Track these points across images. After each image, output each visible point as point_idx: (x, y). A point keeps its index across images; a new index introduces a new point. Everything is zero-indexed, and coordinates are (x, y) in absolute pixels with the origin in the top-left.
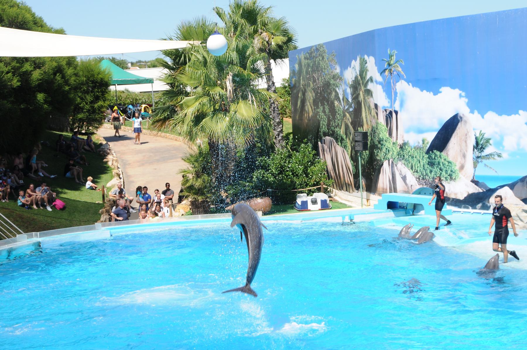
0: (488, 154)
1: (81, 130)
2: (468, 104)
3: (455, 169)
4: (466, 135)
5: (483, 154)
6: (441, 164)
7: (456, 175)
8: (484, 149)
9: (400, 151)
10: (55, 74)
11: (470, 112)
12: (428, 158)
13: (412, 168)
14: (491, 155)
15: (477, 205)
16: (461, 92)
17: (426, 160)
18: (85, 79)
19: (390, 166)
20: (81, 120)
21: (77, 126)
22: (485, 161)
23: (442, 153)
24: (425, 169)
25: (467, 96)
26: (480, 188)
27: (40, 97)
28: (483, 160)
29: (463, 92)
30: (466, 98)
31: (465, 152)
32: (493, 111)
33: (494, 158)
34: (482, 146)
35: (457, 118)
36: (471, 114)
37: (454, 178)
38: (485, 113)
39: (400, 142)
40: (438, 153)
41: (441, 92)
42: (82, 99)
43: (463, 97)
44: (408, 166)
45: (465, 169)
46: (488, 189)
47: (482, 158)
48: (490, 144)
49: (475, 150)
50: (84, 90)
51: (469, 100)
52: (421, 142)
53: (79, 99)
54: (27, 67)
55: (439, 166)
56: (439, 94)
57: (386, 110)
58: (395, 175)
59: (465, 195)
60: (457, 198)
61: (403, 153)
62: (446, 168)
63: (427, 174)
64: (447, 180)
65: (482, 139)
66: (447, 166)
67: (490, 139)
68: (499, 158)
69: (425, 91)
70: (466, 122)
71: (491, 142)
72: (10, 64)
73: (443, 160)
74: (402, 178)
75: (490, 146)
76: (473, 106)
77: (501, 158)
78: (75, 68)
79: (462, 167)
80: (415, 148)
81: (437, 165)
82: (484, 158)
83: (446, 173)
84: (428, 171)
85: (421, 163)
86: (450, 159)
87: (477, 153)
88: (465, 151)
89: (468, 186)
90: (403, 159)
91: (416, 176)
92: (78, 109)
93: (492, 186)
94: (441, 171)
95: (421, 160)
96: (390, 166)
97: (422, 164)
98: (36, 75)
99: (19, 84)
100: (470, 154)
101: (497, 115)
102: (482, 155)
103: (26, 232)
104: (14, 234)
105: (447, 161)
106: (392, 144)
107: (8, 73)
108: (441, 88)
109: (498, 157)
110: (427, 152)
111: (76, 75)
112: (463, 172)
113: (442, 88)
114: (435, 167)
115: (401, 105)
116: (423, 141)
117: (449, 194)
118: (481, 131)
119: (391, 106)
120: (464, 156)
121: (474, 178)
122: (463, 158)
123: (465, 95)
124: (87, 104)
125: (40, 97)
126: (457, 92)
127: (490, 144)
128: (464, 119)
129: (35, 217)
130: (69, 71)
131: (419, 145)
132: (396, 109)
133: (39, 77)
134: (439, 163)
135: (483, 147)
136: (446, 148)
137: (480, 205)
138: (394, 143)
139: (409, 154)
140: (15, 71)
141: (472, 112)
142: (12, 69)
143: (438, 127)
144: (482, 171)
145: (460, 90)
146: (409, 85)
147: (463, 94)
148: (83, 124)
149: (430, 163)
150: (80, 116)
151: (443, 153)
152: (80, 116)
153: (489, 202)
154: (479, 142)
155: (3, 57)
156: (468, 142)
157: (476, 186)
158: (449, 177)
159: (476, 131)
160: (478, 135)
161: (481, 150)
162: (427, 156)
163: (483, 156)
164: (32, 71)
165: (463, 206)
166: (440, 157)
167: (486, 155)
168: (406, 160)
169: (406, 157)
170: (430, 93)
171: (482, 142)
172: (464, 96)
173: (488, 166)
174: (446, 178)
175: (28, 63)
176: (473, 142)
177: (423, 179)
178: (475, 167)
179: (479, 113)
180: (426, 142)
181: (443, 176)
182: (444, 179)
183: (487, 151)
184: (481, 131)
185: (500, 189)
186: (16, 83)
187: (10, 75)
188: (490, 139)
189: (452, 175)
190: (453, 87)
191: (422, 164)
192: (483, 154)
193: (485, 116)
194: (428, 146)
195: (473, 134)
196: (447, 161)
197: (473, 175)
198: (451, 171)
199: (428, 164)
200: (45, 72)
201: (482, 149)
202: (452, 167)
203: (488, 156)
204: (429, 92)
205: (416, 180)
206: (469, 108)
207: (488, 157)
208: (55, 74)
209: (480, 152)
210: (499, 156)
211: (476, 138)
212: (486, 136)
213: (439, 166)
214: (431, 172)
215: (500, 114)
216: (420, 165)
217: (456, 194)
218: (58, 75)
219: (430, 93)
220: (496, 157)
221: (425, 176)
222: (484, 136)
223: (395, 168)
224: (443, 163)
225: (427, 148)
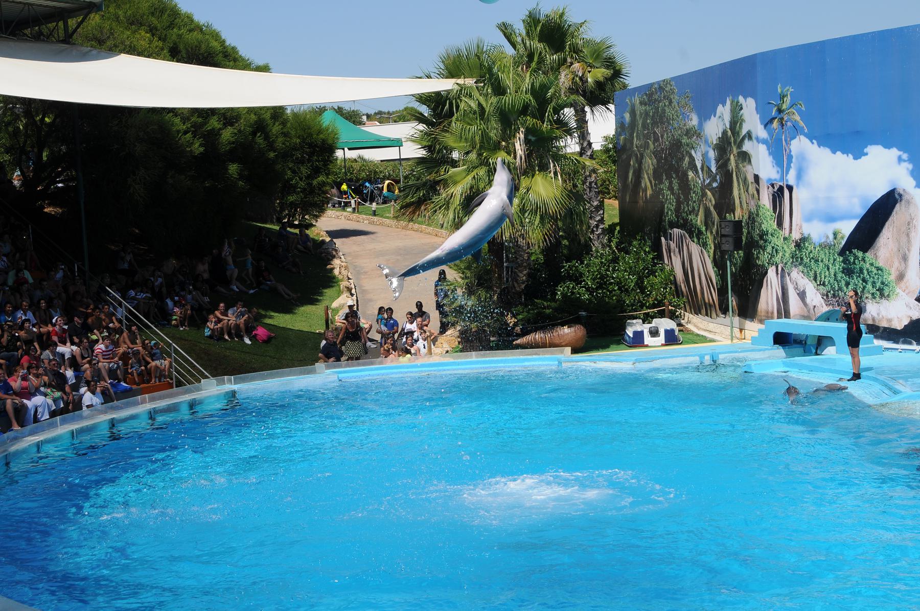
1: (294, 221)
3: (889, 280)
4: (909, 224)
6: (865, 272)
9: (795, 251)
10: (254, 134)
11: (915, 187)
12: (842, 262)
13: (815, 279)
17: (840, 265)
18: (298, 141)
19: (779, 275)
20: (293, 205)
21: (287, 214)
23: (867, 254)
24: (837, 281)
25: (910, 160)
29: (905, 152)
30: (910, 163)
31: (907, 252)
37: (886, 294)
39: (796, 236)
40: (860, 254)
41: (867, 154)
42: (294, 172)
43: (905, 161)
45: (905, 280)
50: (297, 159)
51: (914, 166)
52: (831, 237)
53: (289, 173)
54: (214, 123)
55: (862, 275)
56: (863, 157)
57: (773, 185)
59: (906, 322)
60: (892, 327)
61: (801, 255)
62: (873, 277)
63: (840, 289)
64: (875, 298)
66: (876, 274)
69: (839, 153)
70: (908, 202)
72: (189, 119)
73: (868, 265)
74: (798, 294)
79: (901, 277)
80: (820, 246)
83: (873, 287)
84: (843, 283)
86: (880, 264)
89: (911, 308)
90: (800, 264)
92: (289, 188)
94: (864, 284)
95: (830, 265)
96: (779, 275)
97: (832, 271)
98: (227, 134)
99: (202, 149)
103: (213, 376)
104: (197, 378)
105: (875, 267)
108: (866, 147)
110: (842, 253)
112: (902, 284)
113: (869, 146)
114: (855, 277)
115: (799, 177)
116: (835, 234)
117: (877, 321)
119: (782, 178)
120: (905, 258)
122: (903, 262)
123: (908, 157)
124: (301, 179)
125: (233, 168)
126: (894, 152)
128: (905, 197)
129: (228, 353)
130: (276, 129)
131: (828, 241)
132: (791, 183)
133: (232, 139)
134: (861, 270)
138: (785, 239)
139: (811, 256)
140: (196, 130)
143: (861, 212)
145: (899, 150)
146: (813, 143)
148: (296, 210)
150: (291, 198)
151: (869, 255)
152: (291, 198)
155: (179, 109)
162: (841, 259)
164: (220, 129)
165: (901, 340)
166: (864, 260)
168: (805, 266)
169: (806, 260)
170: (848, 156)
172: (906, 159)
174: (873, 294)
175: (215, 117)
177: (834, 296)
180: (839, 236)
182: (870, 296)
186: (197, 148)
187: (189, 135)
189: (883, 289)
190: (887, 146)
191: (832, 271)
194: (843, 243)
198: (883, 283)
199: (843, 272)
200: (240, 131)
202: (882, 276)
204: (845, 155)
205: (823, 298)
206: (915, 179)
208: (254, 134)
213: (862, 275)
214: (847, 284)
217: (890, 321)
218: (259, 134)
219: (848, 156)
221: (838, 291)
223: (788, 278)
224: (867, 270)
225: (841, 246)
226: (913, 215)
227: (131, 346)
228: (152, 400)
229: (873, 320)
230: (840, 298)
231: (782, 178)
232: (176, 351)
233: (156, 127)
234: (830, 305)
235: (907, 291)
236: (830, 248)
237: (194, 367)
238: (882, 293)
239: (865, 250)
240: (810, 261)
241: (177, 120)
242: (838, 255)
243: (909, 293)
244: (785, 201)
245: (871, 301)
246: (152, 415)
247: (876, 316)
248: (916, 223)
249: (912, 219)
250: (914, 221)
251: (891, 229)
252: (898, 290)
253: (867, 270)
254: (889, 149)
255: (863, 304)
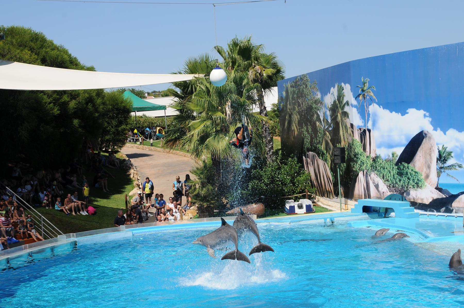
0: (450, 165)
1: (108, 149)
2: (432, 123)
4: (430, 149)
5: (446, 165)
6: (409, 174)
7: (422, 183)
8: (446, 160)
9: (373, 163)
10: (87, 104)
11: (433, 130)
13: (383, 178)
14: (452, 166)
15: (441, 209)
16: (425, 112)
17: (396, 171)
18: (111, 107)
19: (365, 176)
20: (108, 141)
21: (105, 146)
22: (447, 171)
23: (410, 165)
24: (395, 179)
25: (430, 116)
26: (444, 194)
27: (76, 122)
28: (445, 170)
29: (427, 112)
30: (430, 118)
31: (430, 163)
32: (454, 128)
33: (455, 169)
34: (444, 158)
35: (422, 135)
36: (435, 132)
37: (420, 186)
38: (447, 130)
39: (373, 155)
40: (406, 165)
41: (408, 113)
42: (108, 123)
43: (427, 117)
44: (380, 176)
45: (430, 178)
46: (450, 195)
47: (445, 169)
48: (452, 157)
49: (439, 162)
50: (110, 116)
51: (432, 119)
52: (391, 156)
54: (65, 98)
56: (406, 115)
57: (360, 129)
58: (369, 183)
61: (376, 165)
63: (396, 183)
64: (414, 188)
65: (444, 152)
66: (414, 175)
67: (451, 152)
68: (459, 169)
69: (394, 112)
70: (430, 138)
71: (452, 154)
72: (51, 96)
73: (410, 171)
74: (375, 186)
75: (452, 158)
76: (436, 124)
77: (462, 168)
78: (103, 98)
79: (427, 177)
80: (386, 160)
81: (405, 175)
82: (446, 169)
84: (398, 180)
85: (391, 173)
87: (441, 165)
88: (430, 163)
89: (433, 193)
90: (375, 170)
91: (387, 184)
92: (106, 132)
93: (454, 192)
94: (408, 180)
95: (391, 171)
96: (365, 176)
97: (392, 174)
98: (72, 104)
99: (59, 112)
100: (434, 166)
101: (457, 132)
102: (444, 166)
103: (65, 233)
105: (414, 172)
106: (366, 157)
107: (50, 103)
108: (407, 109)
109: (459, 167)
110: (397, 164)
111: (104, 104)
112: (428, 180)
113: (409, 109)
114: (404, 177)
115: (374, 124)
116: (393, 155)
118: (443, 145)
119: (365, 125)
120: (429, 167)
121: (437, 185)
122: (428, 169)
123: (429, 115)
124: (112, 127)
125: (76, 122)
126: (422, 112)
127: (452, 157)
128: (428, 136)
130: (99, 101)
131: (390, 158)
133: (75, 107)
134: (407, 173)
135: (446, 159)
136: (413, 160)
137: (443, 209)
138: (367, 157)
139: (381, 166)
141: (435, 129)
142: (53, 100)
143: (406, 143)
144: (445, 180)
145: (425, 111)
146: (380, 107)
147: (427, 114)
149: (399, 174)
150: (107, 137)
151: (411, 165)
152: (107, 137)
153: (451, 206)
154: (442, 155)
155: (46, 91)
156: (433, 155)
157: (440, 192)
158: (416, 185)
159: (439, 146)
160: (441, 149)
161: (443, 161)
162: (397, 167)
163: (446, 167)
164: (69, 101)
165: (428, 209)
166: (408, 168)
167: (449, 166)
168: (378, 171)
169: (378, 168)
170: (398, 114)
171: (444, 155)
172: (428, 115)
173: (450, 175)
174: (413, 186)
175: (66, 95)
176: (435, 155)
177: (393, 187)
178: (439, 176)
179: (441, 130)
180: (395, 156)
181: (411, 184)
182: (412, 187)
183: (450, 162)
184: (443, 145)
185: (461, 195)
186: (56, 111)
187: (52, 105)
188: (451, 152)
189: (418, 183)
190: (418, 109)
191: (392, 174)
192: (446, 165)
193: (447, 133)
194: (397, 159)
195: (436, 148)
196: (414, 172)
197: (437, 183)
198: (418, 180)
199: (397, 174)
200: (79, 102)
201: (445, 161)
202: (418, 176)
203: (450, 167)
204: (397, 114)
205: (388, 188)
206: (433, 126)
207: (450, 167)
208: (87, 104)
209: (442, 164)
210: (460, 166)
211: (439, 152)
212: (448, 150)
214: (400, 180)
215: (460, 130)
216: (391, 175)
217: (422, 199)
218: (89, 104)
219: (398, 114)
220: (457, 168)
221: (395, 184)
222: (446, 150)
223: (369, 177)
224: (410, 173)
225: (396, 161)
226: (432, 145)
227: (19, 218)
228: (30, 247)
229: (414, 199)
230: (396, 188)
231: (365, 125)
232: (44, 220)
233: (33, 101)
234: (391, 191)
235: (431, 184)
236: (390, 162)
237: (54, 229)
238: (418, 185)
239: (409, 163)
240: (381, 168)
241: (45, 97)
242: (395, 165)
243: (432, 185)
244: (367, 137)
245: (412, 189)
246: (30, 255)
247: (415, 197)
248: (434, 149)
249: (432, 147)
250: (433, 148)
251: (421, 152)
252: (426, 184)
253: (410, 173)
254: (419, 110)
255: (408, 191)
